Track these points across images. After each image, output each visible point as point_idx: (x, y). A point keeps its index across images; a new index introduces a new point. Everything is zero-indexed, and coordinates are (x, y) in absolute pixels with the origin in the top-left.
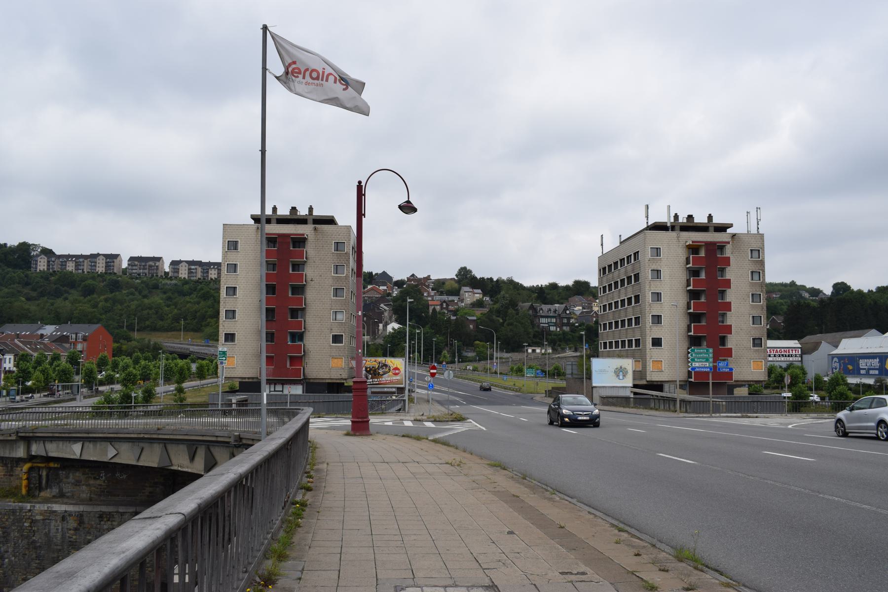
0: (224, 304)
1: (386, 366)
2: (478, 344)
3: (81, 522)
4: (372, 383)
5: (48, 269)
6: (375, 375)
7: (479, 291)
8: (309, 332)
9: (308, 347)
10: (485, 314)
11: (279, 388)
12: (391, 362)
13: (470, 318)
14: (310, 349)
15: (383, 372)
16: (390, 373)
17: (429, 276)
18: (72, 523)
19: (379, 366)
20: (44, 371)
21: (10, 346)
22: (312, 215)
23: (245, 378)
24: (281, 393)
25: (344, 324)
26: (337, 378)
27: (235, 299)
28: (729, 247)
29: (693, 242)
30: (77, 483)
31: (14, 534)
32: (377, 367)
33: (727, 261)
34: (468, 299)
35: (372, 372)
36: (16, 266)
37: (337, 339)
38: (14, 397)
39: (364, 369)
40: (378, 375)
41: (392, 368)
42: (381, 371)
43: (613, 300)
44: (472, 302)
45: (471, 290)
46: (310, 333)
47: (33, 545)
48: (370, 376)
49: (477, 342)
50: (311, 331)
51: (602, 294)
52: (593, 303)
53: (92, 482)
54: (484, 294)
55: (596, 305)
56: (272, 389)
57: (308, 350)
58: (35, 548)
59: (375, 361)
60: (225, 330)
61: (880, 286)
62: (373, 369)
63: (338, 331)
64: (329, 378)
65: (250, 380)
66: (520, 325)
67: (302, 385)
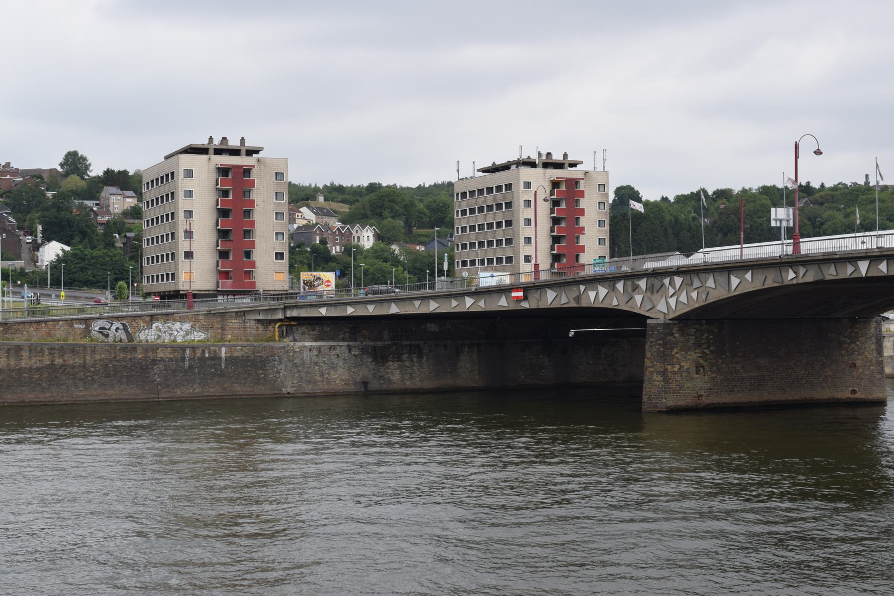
1: (319, 279)
3: (320, 352)
6: (311, 286)
7: (131, 193)
18: (315, 352)
22: (244, 146)
23: (202, 291)
28: (582, 182)
29: (557, 178)
30: (303, 333)
31: (285, 360)
33: (582, 194)
34: (117, 206)
37: (279, 256)
39: (302, 281)
41: (324, 281)
42: (316, 284)
43: (476, 223)
45: (120, 192)
51: (460, 216)
52: (297, 214)
53: (311, 332)
55: (300, 217)
58: (296, 366)
59: (311, 275)
61: (680, 194)
65: (207, 292)
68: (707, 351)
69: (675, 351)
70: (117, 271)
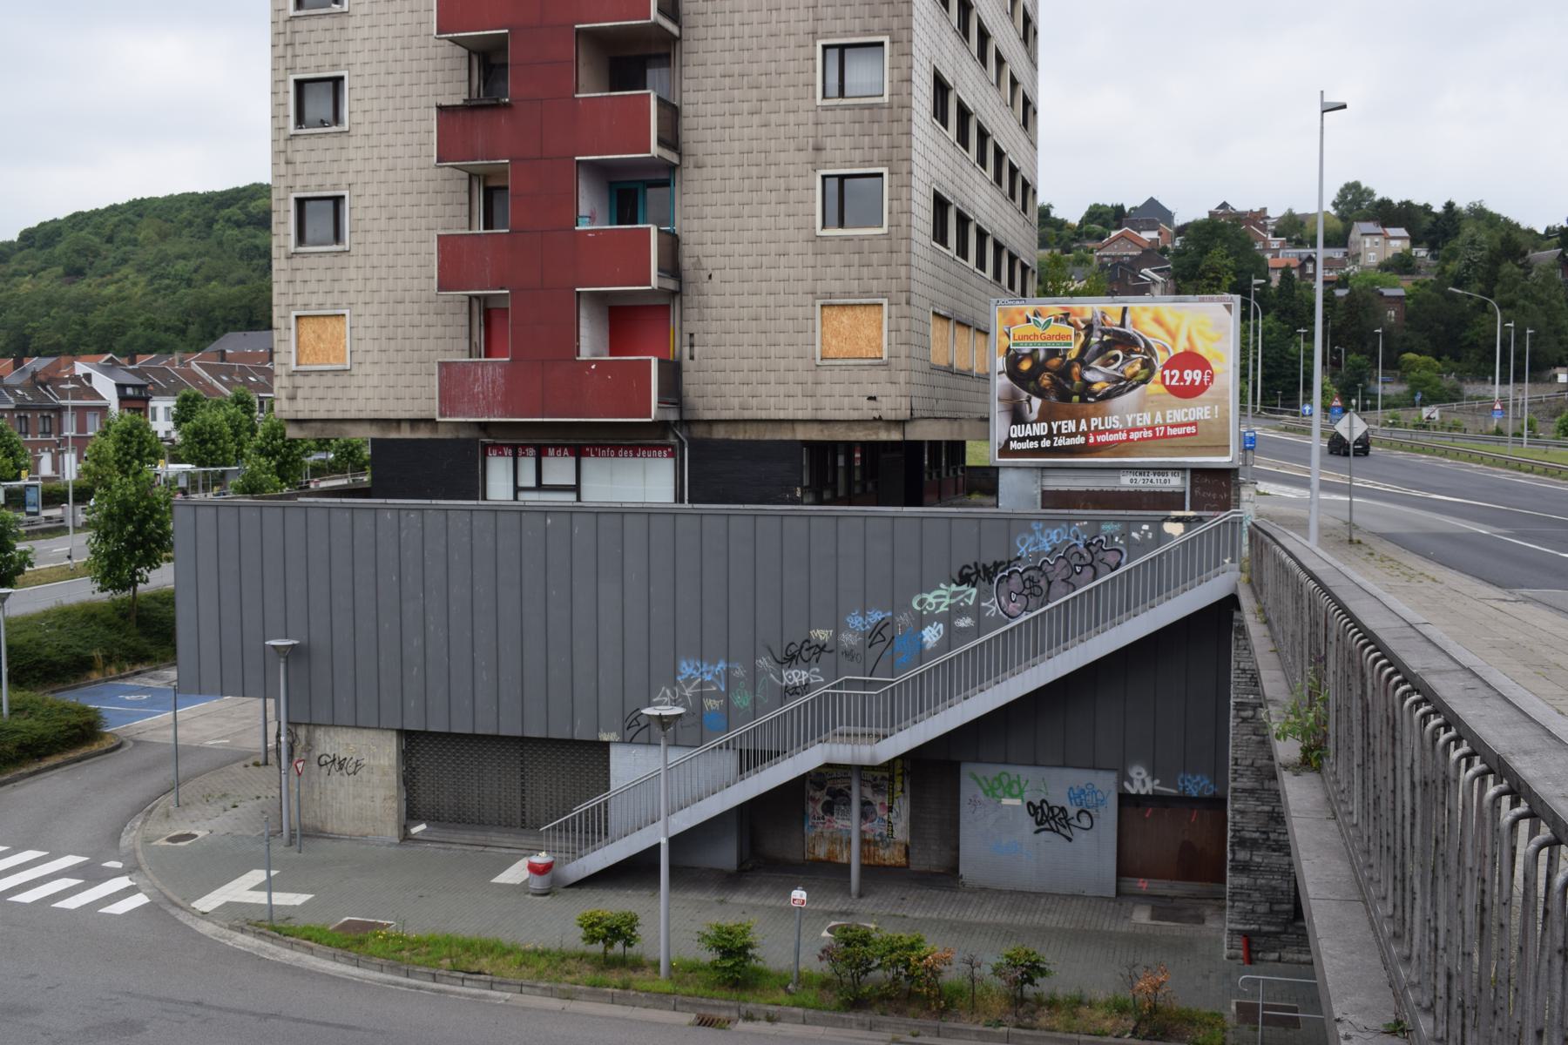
0: (289, 51)
1: (1125, 342)
2: (1411, 362)
4: (1046, 443)
6: (1065, 396)
7: (1402, 232)
8: (698, 167)
9: (697, 250)
10: (1425, 285)
11: (559, 469)
12: (1158, 321)
13: (1387, 292)
14: (707, 263)
15: (1109, 379)
16: (1154, 387)
17: (1264, 210)
19: (1085, 348)
20: (130, 433)
21: (173, 377)
23: (399, 422)
24: (571, 497)
25: (885, 112)
26: (855, 415)
27: (336, 22)
32: (1073, 355)
34: (1372, 254)
35: (1045, 380)
38: (35, 510)
40: (1083, 400)
41: (1161, 358)
42: (1098, 377)
44: (1382, 259)
45: (1380, 230)
46: (706, 172)
48: (1037, 403)
49: (1410, 356)
50: (709, 160)
54: (1415, 242)
56: (528, 479)
57: (698, 266)
59: (1065, 318)
60: (299, 182)
62: (1055, 362)
63: (857, 155)
64: (808, 415)
66: (1534, 306)
67: (670, 455)
70: (1270, 363)
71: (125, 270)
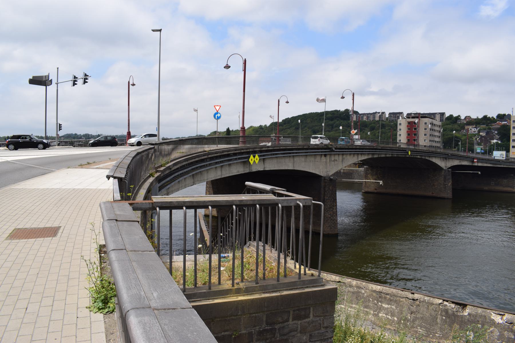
5: (356, 120)
31: (356, 173)
36: (344, 119)
47: (359, 175)
68: (379, 176)
69: (369, 175)
71: (306, 128)
